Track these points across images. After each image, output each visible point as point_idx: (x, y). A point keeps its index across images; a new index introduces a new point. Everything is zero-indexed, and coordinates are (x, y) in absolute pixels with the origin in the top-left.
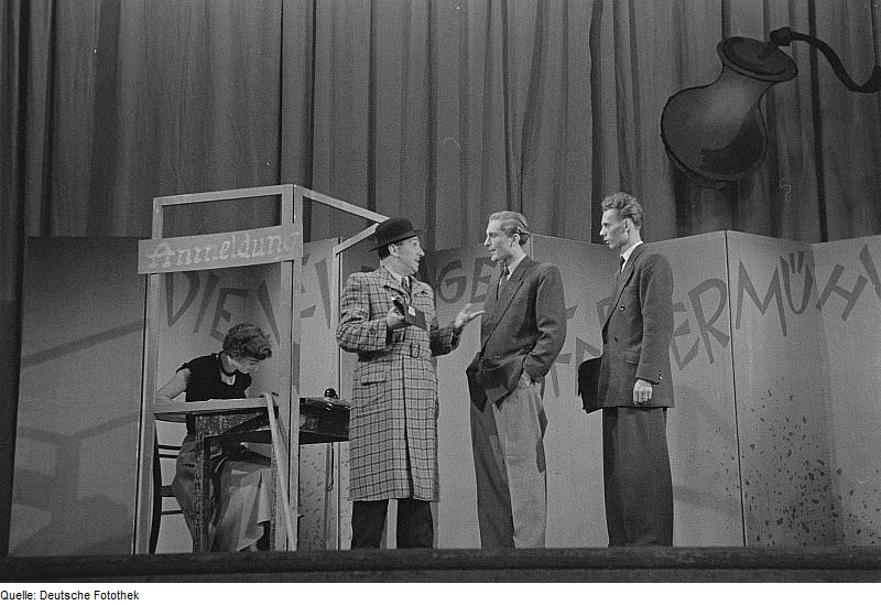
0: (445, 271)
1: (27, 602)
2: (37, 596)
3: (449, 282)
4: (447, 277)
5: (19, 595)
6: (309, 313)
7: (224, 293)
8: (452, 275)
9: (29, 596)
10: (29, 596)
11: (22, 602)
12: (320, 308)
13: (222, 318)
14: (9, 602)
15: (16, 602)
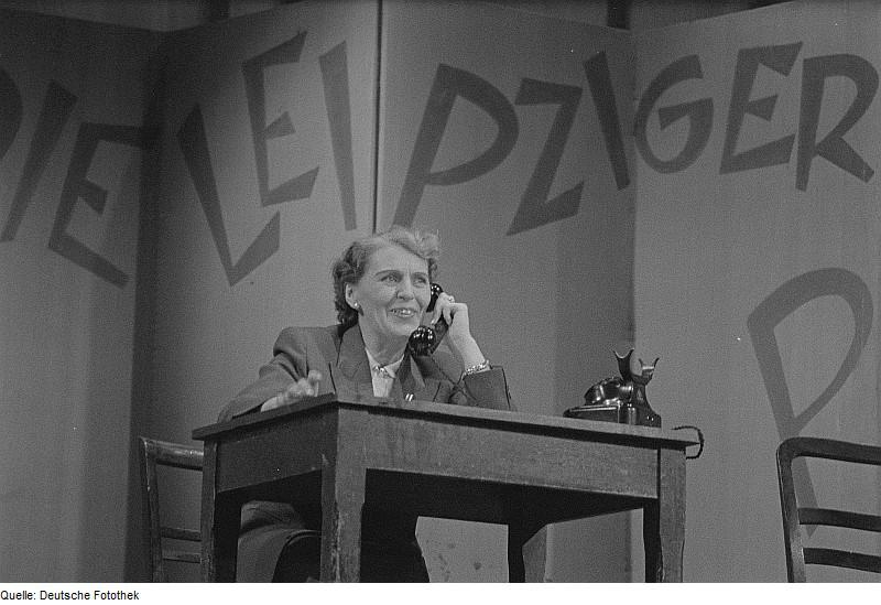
0: (657, 88)
1: (27, 602)
2: (37, 596)
3: (669, 116)
4: (664, 101)
5: (19, 595)
6: (301, 187)
7: (89, 139)
8: (682, 92)
9: (29, 596)
10: (29, 596)
11: (22, 602)
12: (327, 187)
13: (81, 203)
14: (9, 602)
15: (16, 602)
